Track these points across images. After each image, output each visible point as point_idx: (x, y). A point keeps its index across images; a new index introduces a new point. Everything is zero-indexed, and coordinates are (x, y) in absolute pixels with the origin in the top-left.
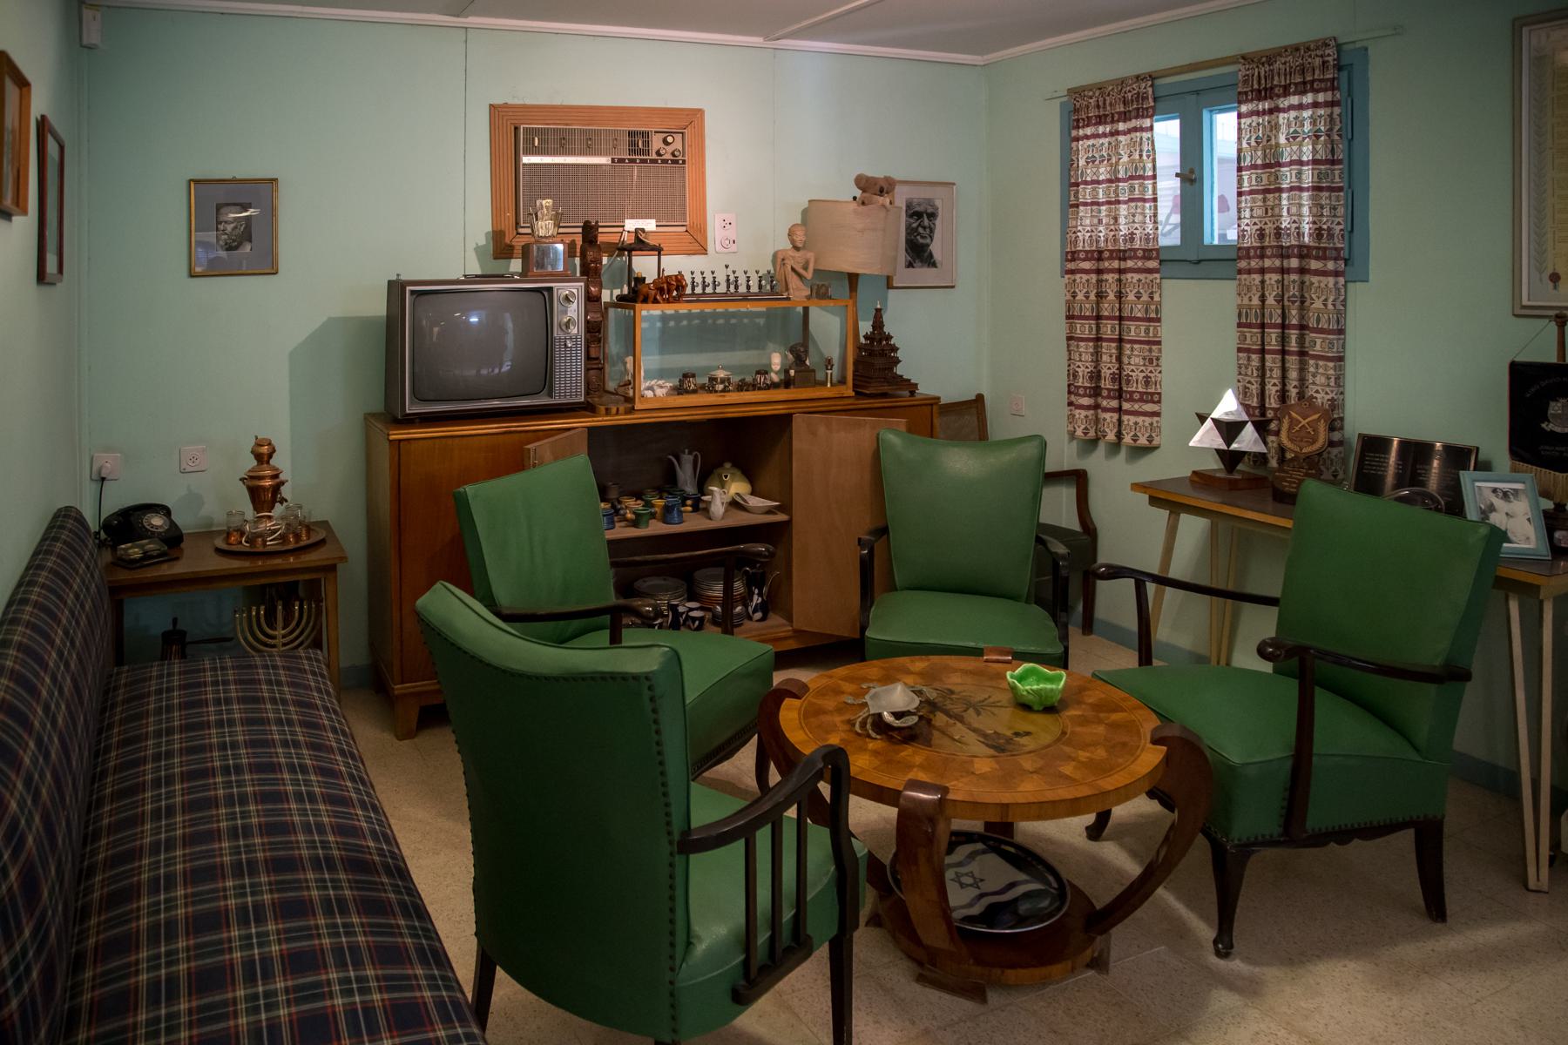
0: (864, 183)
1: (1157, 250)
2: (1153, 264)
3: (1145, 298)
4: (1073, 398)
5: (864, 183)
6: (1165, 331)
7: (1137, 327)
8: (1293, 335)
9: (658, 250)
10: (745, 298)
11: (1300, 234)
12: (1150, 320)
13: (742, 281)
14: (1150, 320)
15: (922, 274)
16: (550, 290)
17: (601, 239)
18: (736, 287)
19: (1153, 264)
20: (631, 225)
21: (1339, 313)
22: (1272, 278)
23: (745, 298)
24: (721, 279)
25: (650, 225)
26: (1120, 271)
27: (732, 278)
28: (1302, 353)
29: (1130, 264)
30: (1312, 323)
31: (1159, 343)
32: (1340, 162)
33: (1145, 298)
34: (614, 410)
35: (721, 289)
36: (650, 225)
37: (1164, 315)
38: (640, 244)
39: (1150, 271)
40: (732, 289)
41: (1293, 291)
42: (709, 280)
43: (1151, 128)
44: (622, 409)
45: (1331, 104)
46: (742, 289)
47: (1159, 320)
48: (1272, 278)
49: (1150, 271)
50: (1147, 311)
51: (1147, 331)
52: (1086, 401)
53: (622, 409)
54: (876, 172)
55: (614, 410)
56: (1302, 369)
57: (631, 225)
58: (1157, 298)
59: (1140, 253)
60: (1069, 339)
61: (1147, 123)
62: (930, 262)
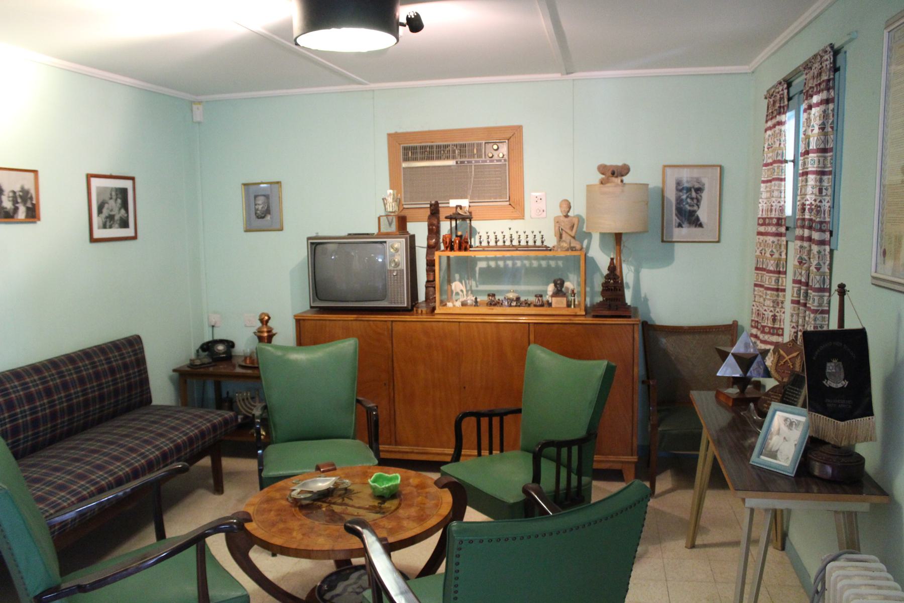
1: (785, 219)
2: (783, 230)
3: (776, 255)
7: (770, 278)
10: (516, 248)
11: (782, 210)
12: (779, 272)
14: (779, 272)
20: (453, 203)
23: (516, 248)
25: (465, 203)
27: (515, 237)
36: (465, 203)
39: (780, 235)
45: (827, 101)
50: (777, 265)
51: (777, 280)
57: (453, 203)
59: (775, 221)
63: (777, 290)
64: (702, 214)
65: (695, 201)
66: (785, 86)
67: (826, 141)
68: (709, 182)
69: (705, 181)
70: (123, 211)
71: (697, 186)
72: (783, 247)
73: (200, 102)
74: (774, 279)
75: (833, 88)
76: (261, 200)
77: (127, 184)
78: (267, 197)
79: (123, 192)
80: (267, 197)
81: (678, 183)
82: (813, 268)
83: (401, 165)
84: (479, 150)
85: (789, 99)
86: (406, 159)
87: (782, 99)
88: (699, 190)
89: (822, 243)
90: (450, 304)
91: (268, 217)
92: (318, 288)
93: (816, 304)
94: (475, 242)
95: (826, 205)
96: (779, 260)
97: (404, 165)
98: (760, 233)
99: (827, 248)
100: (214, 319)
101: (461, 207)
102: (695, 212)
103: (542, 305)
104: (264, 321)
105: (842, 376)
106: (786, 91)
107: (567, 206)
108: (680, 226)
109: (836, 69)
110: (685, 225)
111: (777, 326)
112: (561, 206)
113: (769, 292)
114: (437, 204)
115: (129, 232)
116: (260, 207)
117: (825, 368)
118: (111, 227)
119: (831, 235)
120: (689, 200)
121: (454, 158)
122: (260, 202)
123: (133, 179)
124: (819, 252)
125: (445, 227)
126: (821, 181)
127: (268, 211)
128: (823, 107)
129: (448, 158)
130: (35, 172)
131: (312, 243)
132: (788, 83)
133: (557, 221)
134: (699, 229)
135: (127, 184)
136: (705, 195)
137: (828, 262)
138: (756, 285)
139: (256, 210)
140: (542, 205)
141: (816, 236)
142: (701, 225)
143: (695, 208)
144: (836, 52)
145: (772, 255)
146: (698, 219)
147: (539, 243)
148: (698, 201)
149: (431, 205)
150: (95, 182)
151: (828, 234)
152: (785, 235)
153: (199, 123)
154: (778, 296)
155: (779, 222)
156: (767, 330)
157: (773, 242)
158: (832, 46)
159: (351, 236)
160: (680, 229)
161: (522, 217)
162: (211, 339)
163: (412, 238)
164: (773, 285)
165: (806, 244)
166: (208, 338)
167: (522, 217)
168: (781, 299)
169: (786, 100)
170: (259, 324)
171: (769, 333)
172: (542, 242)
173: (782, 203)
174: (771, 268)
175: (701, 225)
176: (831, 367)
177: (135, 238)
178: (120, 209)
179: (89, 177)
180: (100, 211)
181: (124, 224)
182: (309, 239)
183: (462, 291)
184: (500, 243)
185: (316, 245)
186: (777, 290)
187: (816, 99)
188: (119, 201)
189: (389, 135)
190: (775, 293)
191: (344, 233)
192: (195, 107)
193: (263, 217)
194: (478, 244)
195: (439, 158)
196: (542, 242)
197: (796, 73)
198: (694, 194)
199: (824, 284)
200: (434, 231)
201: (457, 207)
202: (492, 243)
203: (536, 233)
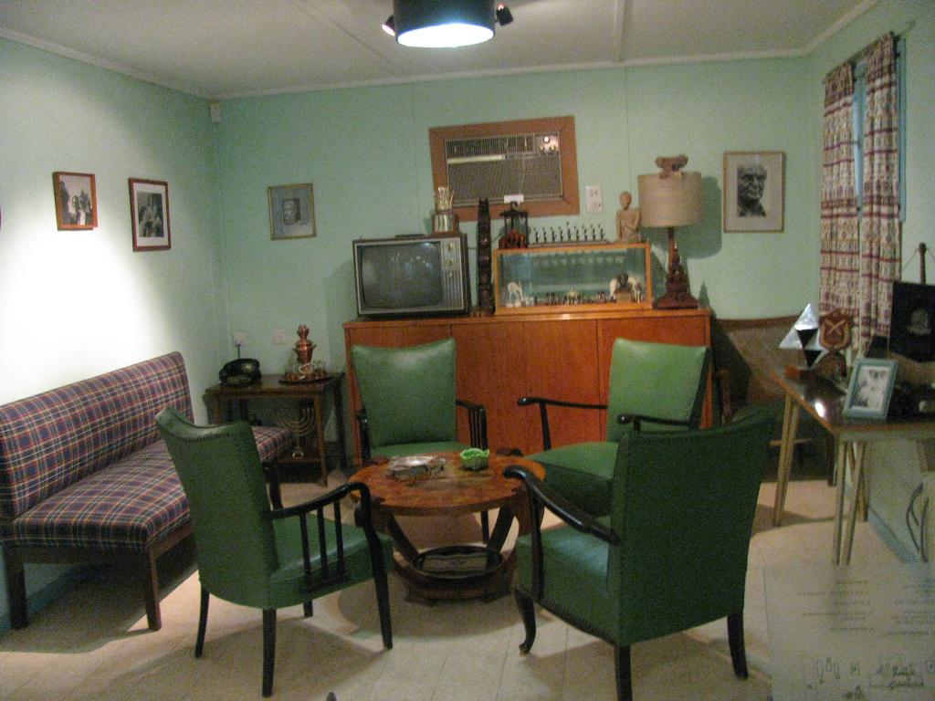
0: (662, 162)
2: (853, 210)
3: (849, 236)
5: (662, 162)
9: (525, 214)
12: (852, 253)
14: (852, 253)
15: (753, 221)
16: (439, 243)
19: (853, 210)
25: (520, 198)
36: (520, 198)
42: (557, 233)
45: (890, 85)
48: (884, 222)
54: (672, 152)
55: (478, 314)
57: (508, 199)
59: (845, 202)
62: (760, 212)
63: (852, 271)
64: (765, 202)
65: (758, 189)
66: (850, 67)
67: (890, 122)
68: (772, 170)
69: (767, 168)
70: (158, 219)
71: (758, 173)
72: (855, 228)
73: (217, 101)
74: (847, 261)
75: (895, 71)
76: (289, 205)
77: (160, 189)
78: (296, 201)
79: (157, 198)
81: (740, 171)
82: (884, 240)
83: (445, 162)
84: (530, 144)
85: (854, 80)
86: (452, 155)
87: (847, 81)
88: (762, 177)
90: (510, 305)
92: (366, 296)
93: (888, 273)
94: (532, 239)
95: (895, 181)
96: (852, 240)
97: (452, 161)
98: (824, 217)
99: (896, 221)
100: (240, 338)
101: (516, 203)
102: (758, 200)
103: (605, 302)
104: (303, 333)
106: (850, 73)
107: (627, 199)
109: (896, 55)
110: (749, 214)
111: (852, 307)
112: (621, 198)
113: (843, 273)
114: (486, 202)
115: (162, 241)
116: (289, 212)
118: (149, 236)
119: (899, 208)
121: (503, 152)
123: (165, 184)
124: (889, 225)
125: (497, 226)
126: (887, 158)
128: (886, 90)
129: (496, 153)
130: (92, 177)
132: (852, 64)
133: (620, 216)
134: (762, 218)
135: (160, 189)
136: (767, 183)
137: (897, 234)
138: (822, 268)
140: (598, 199)
141: (884, 210)
142: (764, 214)
143: (758, 196)
144: (896, 39)
146: (761, 208)
147: (598, 237)
148: (761, 189)
149: (480, 202)
150: (138, 188)
151: (896, 208)
153: (217, 124)
154: (852, 277)
157: (845, 224)
158: (892, 33)
159: (399, 237)
160: (743, 218)
161: (577, 211)
162: (236, 358)
163: (464, 239)
164: (847, 266)
165: (875, 219)
166: (233, 357)
167: (577, 211)
168: (855, 280)
169: (851, 82)
170: (298, 338)
172: (602, 237)
173: (852, 184)
174: (844, 250)
175: (764, 214)
177: (168, 247)
178: (156, 217)
179: (131, 181)
180: (140, 219)
181: (159, 233)
182: (354, 242)
183: (518, 292)
184: (558, 239)
185: (363, 250)
186: (852, 271)
187: (878, 83)
188: (155, 207)
189: (434, 132)
190: (850, 275)
191: (393, 236)
192: (212, 106)
194: (535, 241)
195: (487, 153)
196: (602, 237)
197: (858, 56)
198: (756, 182)
199: (895, 253)
200: (484, 231)
201: (512, 203)
203: (595, 226)
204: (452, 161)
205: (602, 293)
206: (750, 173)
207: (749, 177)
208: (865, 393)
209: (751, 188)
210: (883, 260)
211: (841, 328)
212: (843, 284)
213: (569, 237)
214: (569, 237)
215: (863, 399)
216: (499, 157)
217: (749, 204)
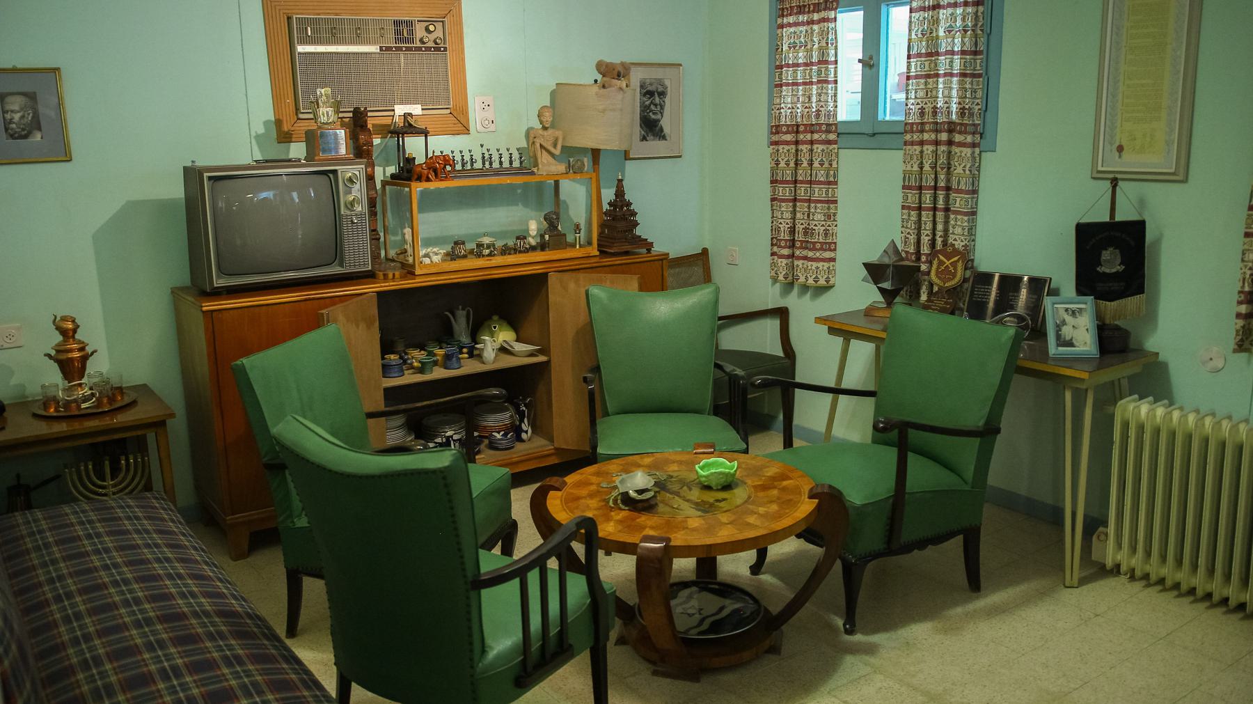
2: (832, 137)
3: (826, 165)
4: (775, 249)
6: (841, 192)
8: (941, 195)
9: (425, 133)
10: (497, 173)
12: (829, 183)
13: (495, 157)
14: (829, 183)
16: (335, 172)
17: (370, 123)
18: (491, 164)
20: (400, 110)
21: (974, 177)
22: (929, 149)
23: (497, 173)
24: (478, 157)
25: (416, 110)
26: (812, 142)
27: (487, 156)
28: (947, 210)
29: (816, 136)
30: (954, 186)
31: (835, 202)
32: (980, 53)
33: (826, 165)
34: (391, 276)
35: (478, 165)
37: (841, 177)
38: (409, 128)
39: (829, 142)
40: (487, 165)
41: (942, 160)
42: (467, 158)
43: (835, 19)
44: (397, 274)
46: (496, 165)
47: (836, 183)
49: (829, 142)
52: (786, 252)
53: (397, 274)
55: (391, 276)
56: (946, 222)
57: (400, 110)
58: (835, 165)
59: (824, 127)
60: (773, 200)
61: (832, 14)
63: (828, 202)
64: (666, 124)
69: (667, 83)
71: (660, 89)
78: (31, 97)
80: (31, 97)
88: (662, 94)
89: (974, 145)
91: (38, 136)
97: (301, 49)
101: (410, 115)
105: (1119, 261)
108: (644, 139)
110: (650, 137)
116: (17, 117)
117: (1100, 255)
120: (653, 107)
122: (16, 108)
127: (36, 124)
131: (210, 178)
136: (667, 100)
139: (7, 123)
140: (490, 114)
142: (664, 138)
143: (659, 116)
145: (822, 165)
146: (662, 130)
148: (662, 107)
152: (835, 142)
154: (829, 208)
155: (829, 128)
156: (818, 246)
164: (823, 197)
171: (822, 249)
175: (664, 138)
176: (1106, 255)
186: (828, 202)
193: (26, 137)
198: (657, 100)
202: (506, 165)
203: (503, 151)
204: (301, 49)
205: (522, 238)
206: (650, 88)
207: (650, 94)
208: (1067, 332)
209: (653, 107)
210: (959, 191)
211: (954, 264)
212: (819, 217)
213: (511, 163)
214: (511, 163)
215: (1068, 338)
216: (374, 49)
217: (651, 127)
